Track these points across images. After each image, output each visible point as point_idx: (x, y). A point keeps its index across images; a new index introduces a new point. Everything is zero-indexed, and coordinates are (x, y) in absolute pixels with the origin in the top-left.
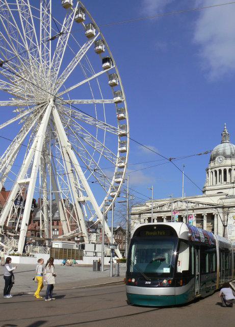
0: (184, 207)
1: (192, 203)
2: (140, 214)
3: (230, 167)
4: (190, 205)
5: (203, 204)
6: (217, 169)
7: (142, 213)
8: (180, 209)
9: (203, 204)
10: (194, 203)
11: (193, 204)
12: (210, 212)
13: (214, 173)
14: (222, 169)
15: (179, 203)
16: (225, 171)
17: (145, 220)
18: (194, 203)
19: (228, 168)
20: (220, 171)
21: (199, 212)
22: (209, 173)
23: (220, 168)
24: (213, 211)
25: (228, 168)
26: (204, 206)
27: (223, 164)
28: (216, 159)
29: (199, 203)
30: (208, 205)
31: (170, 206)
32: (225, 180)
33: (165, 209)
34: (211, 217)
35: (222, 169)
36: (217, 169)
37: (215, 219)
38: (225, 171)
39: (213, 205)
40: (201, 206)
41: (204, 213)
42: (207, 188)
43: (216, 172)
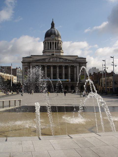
0: (58, 61)
1: (63, 59)
3: (58, 42)
4: (61, 60)
5: (69, 60)
8: (56, 62)
10: (64, 59)
11: (63, 60)
12: (73, 65)
13: (49, 43)
15: (55, 59)
19: (57, 42)
20: (53, 43)
22: (47, 43)
23: (53, 41)
25: (57, 42)
26: (70, 62)
28: (51, 36)
31: (49, 59)
33: (47, 61)
34: (73, 67)
35: (54, 42)
36: (52, 42)
37: (75, 69)
38: (56, 43)
39: (74, 61)
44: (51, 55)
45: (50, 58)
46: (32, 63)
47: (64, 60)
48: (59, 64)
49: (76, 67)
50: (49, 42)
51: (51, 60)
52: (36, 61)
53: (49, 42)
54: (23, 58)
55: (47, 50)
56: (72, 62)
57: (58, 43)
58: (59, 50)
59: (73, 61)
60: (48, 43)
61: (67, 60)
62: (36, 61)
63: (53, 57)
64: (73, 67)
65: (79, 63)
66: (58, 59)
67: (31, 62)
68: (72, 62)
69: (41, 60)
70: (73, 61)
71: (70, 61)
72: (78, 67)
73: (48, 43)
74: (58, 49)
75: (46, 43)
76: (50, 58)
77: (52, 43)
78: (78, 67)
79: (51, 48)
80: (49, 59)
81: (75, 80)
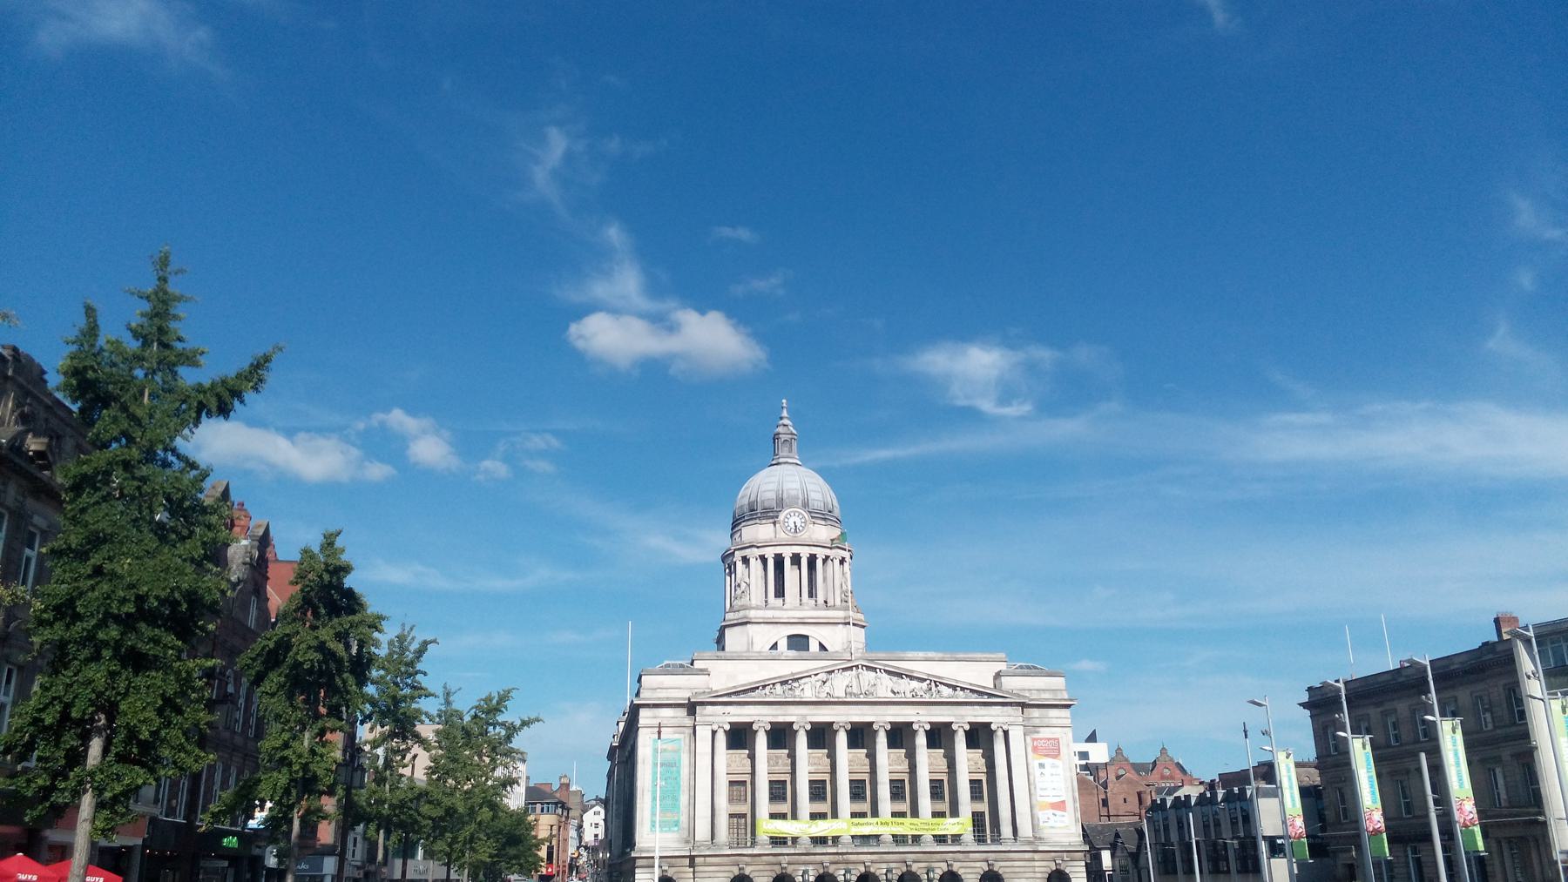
0: (883, 693)
1: (912, 678)
2: (691, 708)
4: (906, 686)
5: (954, 688)
6: (787, 553)
7: (702, 704)
9: (954, 688)
10: (923, 680)
11: (915, 684)
14: (805, 553)
16: (812, 560)
17: (714, 733)
18: (923, 680)
19: (820, 553)
20: (796, 559)
21: (941, 715)
22: (752, 561)
24: (995, 717)
26: (961, 696)
27: (804, 536)
28: (782, 516)
35: (805, 553)
36: (787, 553)
38: (812, 560)
41: (961, 718)
42: (752, 614)
43: (779, 561)
44: (783, 644)
46: (709, 708)
49: (1006, 733)
50: (769, 553)
51: (839, 685)
52: (737, 693)
53: (769, 553)
55: (757, 608)
56: (974, 698)
58: (834, 607)
59: (981, 693)
60: (764, 559)
61: (942, 688)
62: (737, 693)
63: (850, 668)
64: (980, 736)
65: (1023, 705)
67: (702, 704)
70: (981, 693)
71: (963, 689)
72: (1016, 735)
73: (764, 559)
75: (745, 560)
76: (830, 672)
77: (787, 562)
79: (780, 592)
80: (823, 676)
81: (1006, 830)
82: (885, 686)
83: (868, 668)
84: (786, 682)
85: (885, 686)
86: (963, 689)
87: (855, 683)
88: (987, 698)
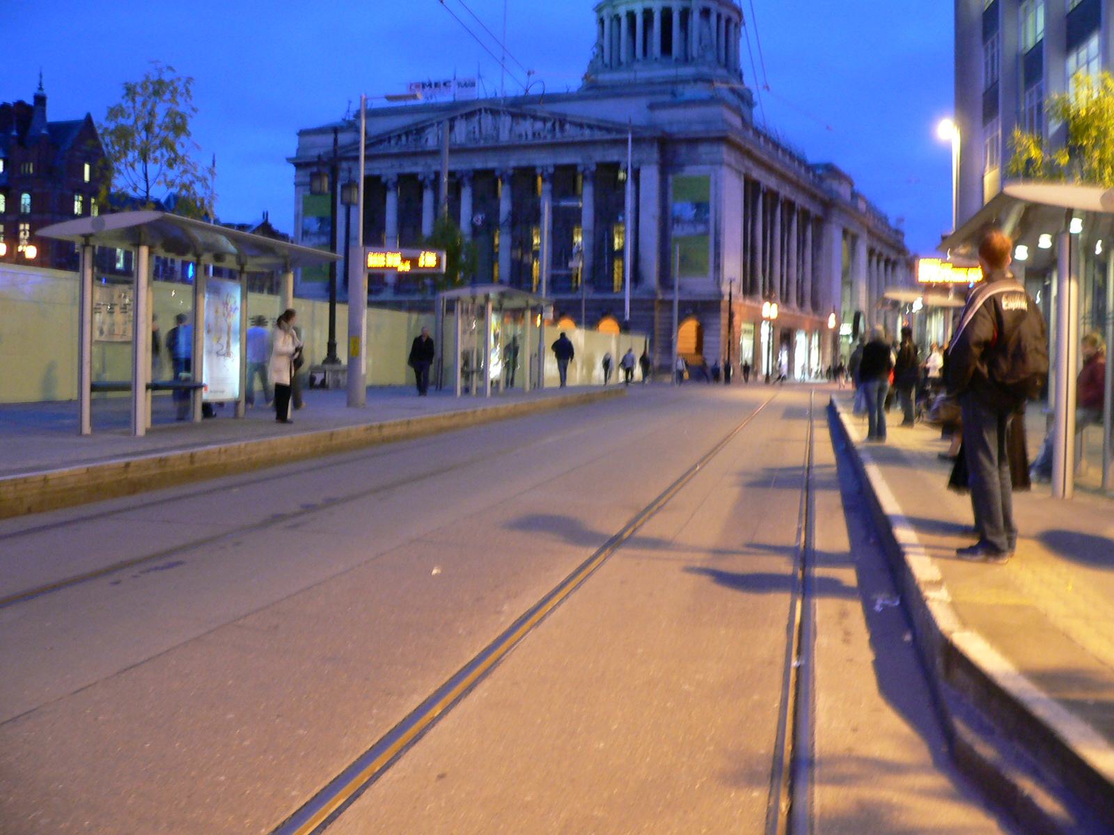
0: (504, 137)
4: (526, 127)
5: (581, 126)
9: (581, 126)
11: (539, 125)
15: (487, 120)
21: (567, 158)
26: (587, 134)
29: (562, 121)
30: (600, 128)
32: (666, 47)
40: (571, 132)
45: (452, 120)
47: (549, 125)
48: (514, 161)
51: (461, 132)
54: (302, 133)
56: (598, 135)
57: (685, 14)
59: (608, 130)
66: (506, 121)
68: (598, 135)
69: (393, 142)
71: (591, 127)
74: (686, 59)
78: (650, 176)
82: (506, 129)
83: (495, 112)
84: (407, 134)
85: (506, 129)
86: (591, 127)
87: (477, 130)
88: (615, 134)
